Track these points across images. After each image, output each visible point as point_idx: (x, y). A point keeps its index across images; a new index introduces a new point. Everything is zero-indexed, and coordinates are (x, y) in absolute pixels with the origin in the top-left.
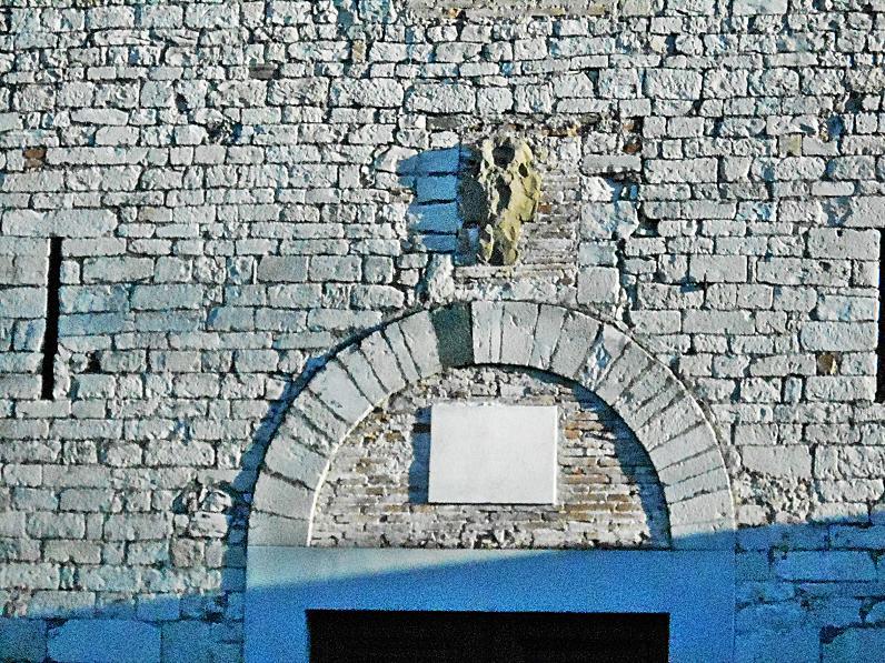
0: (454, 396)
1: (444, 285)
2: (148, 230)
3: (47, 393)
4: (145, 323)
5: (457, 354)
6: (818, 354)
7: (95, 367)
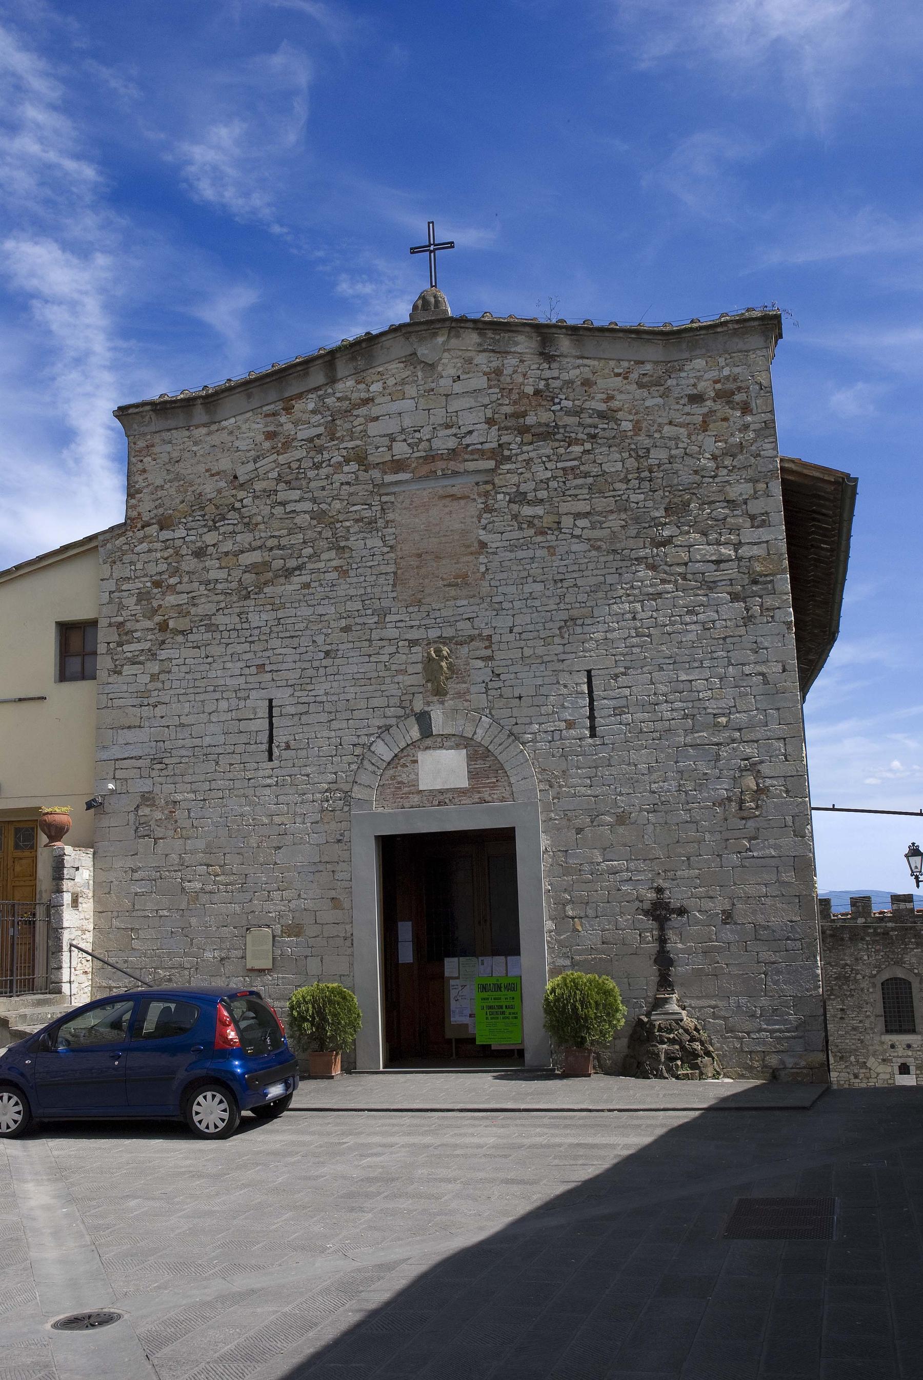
0: (428, 748)
1: (418, 706)
3: (271, 760)
4: (306, 729)
5: (426, 731)
6: (565, 721)
7: (288, 747)
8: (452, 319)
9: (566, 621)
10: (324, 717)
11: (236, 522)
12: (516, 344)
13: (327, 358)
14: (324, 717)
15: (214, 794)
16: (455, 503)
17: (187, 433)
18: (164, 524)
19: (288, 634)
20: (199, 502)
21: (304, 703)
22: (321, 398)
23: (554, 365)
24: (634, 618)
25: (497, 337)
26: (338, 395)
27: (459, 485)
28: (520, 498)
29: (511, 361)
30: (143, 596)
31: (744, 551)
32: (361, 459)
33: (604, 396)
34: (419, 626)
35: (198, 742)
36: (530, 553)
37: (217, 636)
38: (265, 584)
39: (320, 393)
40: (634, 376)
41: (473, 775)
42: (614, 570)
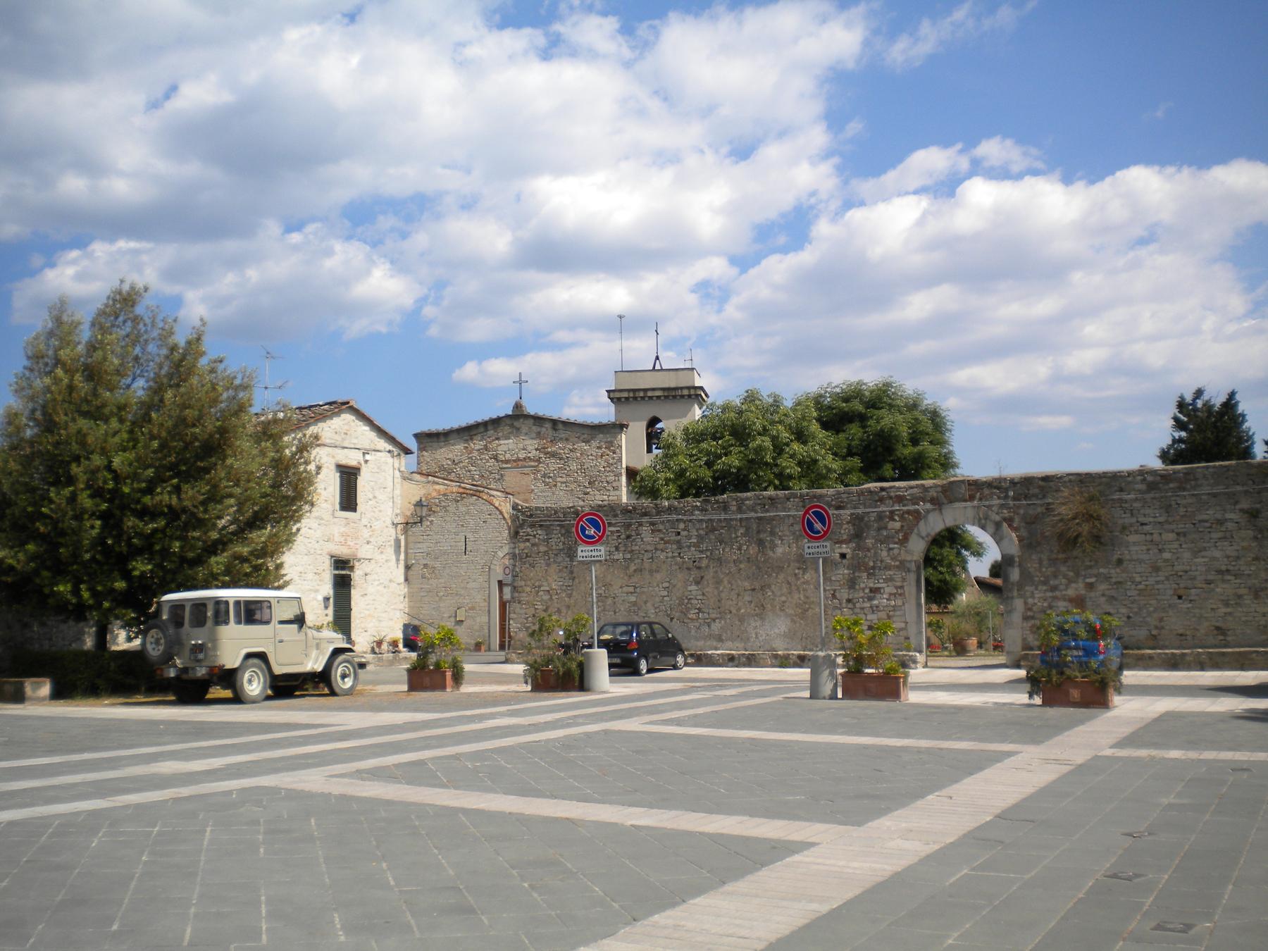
14: (482, 542)
20: (442, 468)
27: (526, 470)
28: (544, 476)
29: (544, 429)
31: (610, 498)
32: (495, 458)
40: (582, 438)
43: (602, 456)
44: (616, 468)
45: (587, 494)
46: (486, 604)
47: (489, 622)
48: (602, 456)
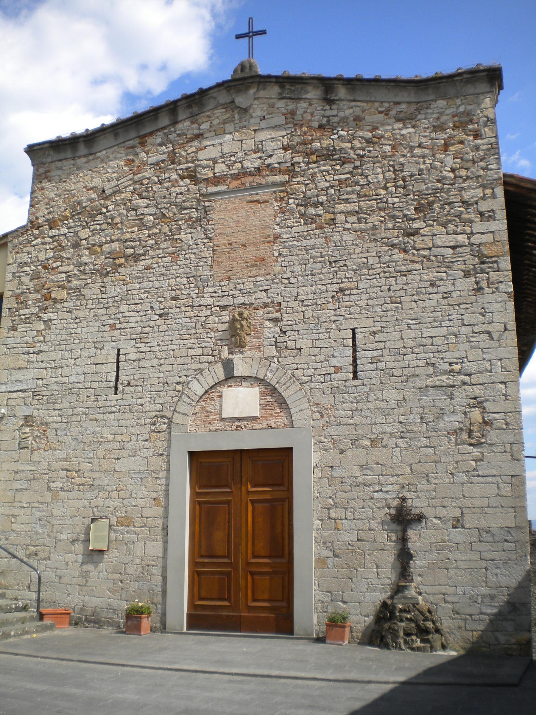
1: (225, 354)
2: (143, 345)
3: (116, 393)
6: (334, 367)
7: (129, 384)
8: (260, 76)
9: (337, 292)
10: (156, 362)
11: (102, 222)
12: (307, 92)
13: (171, 106)
14: (156, 362)
15: (74, 418)
16: (259, 206)
17: (72, 162)
18: (52, 224)
19: (133, 302)
21: (142, 352)
22: (166, 135)
23: (334, 107)
24: (389, 289)
25: (293, 88)
26: (178, 132)
28: (306, 202)
29: (303, 105)
30: (35, 276)
31: (476, 239)
33: (370, 128)
34: (229, 295)
35: (65, 380)
36: (312, 242)
37: (84, 302)
38: (120, 265)
39: (165, 131)
40: (393, 113)
41: (263, 407)
42: (374, 254)
43: (446, 146)
44: (485, 169)
45: (415, 233)
46: (160, 511)
47: (165, 557)
48: (446, 146)
